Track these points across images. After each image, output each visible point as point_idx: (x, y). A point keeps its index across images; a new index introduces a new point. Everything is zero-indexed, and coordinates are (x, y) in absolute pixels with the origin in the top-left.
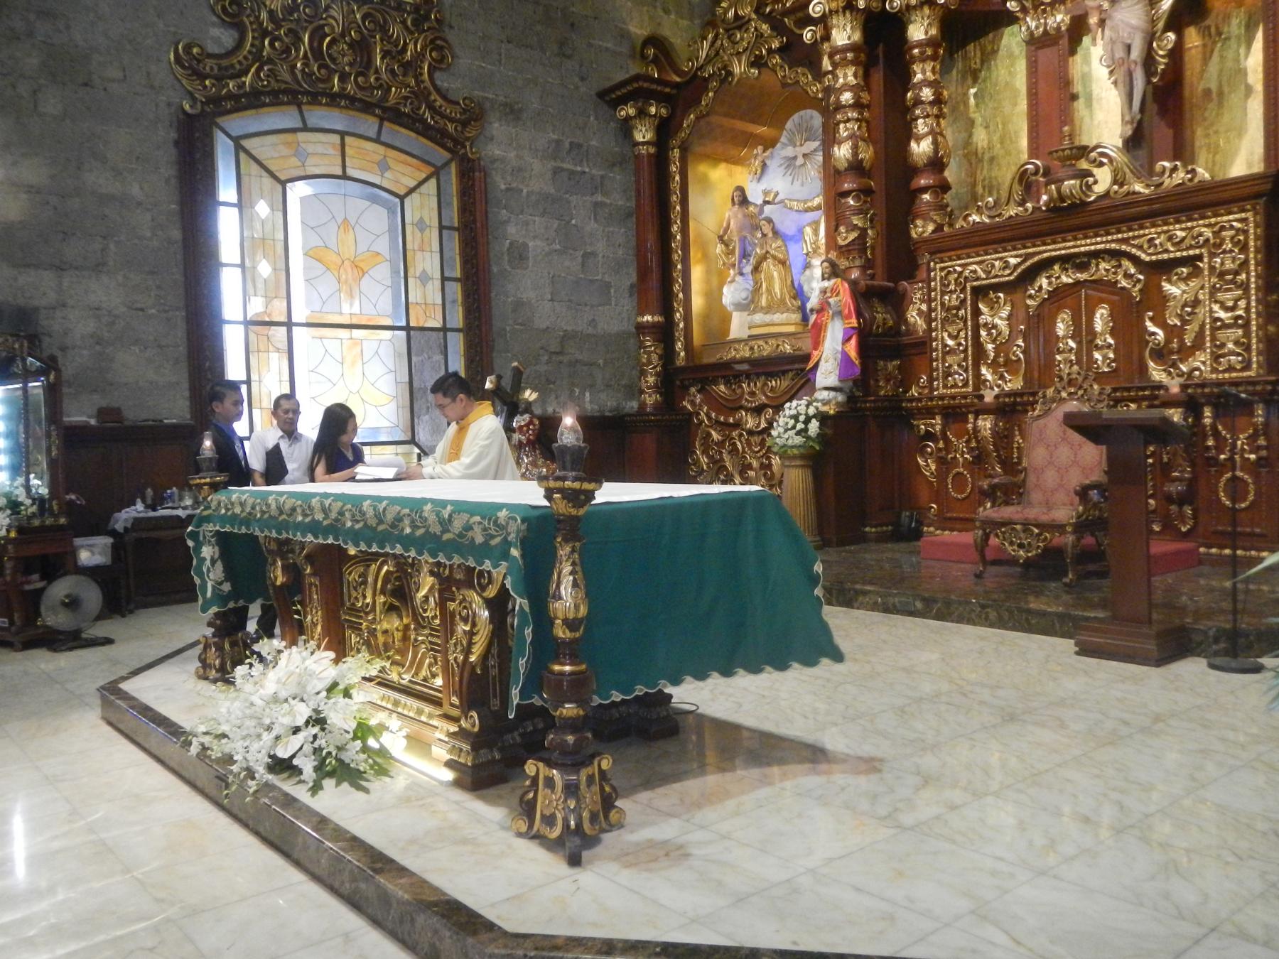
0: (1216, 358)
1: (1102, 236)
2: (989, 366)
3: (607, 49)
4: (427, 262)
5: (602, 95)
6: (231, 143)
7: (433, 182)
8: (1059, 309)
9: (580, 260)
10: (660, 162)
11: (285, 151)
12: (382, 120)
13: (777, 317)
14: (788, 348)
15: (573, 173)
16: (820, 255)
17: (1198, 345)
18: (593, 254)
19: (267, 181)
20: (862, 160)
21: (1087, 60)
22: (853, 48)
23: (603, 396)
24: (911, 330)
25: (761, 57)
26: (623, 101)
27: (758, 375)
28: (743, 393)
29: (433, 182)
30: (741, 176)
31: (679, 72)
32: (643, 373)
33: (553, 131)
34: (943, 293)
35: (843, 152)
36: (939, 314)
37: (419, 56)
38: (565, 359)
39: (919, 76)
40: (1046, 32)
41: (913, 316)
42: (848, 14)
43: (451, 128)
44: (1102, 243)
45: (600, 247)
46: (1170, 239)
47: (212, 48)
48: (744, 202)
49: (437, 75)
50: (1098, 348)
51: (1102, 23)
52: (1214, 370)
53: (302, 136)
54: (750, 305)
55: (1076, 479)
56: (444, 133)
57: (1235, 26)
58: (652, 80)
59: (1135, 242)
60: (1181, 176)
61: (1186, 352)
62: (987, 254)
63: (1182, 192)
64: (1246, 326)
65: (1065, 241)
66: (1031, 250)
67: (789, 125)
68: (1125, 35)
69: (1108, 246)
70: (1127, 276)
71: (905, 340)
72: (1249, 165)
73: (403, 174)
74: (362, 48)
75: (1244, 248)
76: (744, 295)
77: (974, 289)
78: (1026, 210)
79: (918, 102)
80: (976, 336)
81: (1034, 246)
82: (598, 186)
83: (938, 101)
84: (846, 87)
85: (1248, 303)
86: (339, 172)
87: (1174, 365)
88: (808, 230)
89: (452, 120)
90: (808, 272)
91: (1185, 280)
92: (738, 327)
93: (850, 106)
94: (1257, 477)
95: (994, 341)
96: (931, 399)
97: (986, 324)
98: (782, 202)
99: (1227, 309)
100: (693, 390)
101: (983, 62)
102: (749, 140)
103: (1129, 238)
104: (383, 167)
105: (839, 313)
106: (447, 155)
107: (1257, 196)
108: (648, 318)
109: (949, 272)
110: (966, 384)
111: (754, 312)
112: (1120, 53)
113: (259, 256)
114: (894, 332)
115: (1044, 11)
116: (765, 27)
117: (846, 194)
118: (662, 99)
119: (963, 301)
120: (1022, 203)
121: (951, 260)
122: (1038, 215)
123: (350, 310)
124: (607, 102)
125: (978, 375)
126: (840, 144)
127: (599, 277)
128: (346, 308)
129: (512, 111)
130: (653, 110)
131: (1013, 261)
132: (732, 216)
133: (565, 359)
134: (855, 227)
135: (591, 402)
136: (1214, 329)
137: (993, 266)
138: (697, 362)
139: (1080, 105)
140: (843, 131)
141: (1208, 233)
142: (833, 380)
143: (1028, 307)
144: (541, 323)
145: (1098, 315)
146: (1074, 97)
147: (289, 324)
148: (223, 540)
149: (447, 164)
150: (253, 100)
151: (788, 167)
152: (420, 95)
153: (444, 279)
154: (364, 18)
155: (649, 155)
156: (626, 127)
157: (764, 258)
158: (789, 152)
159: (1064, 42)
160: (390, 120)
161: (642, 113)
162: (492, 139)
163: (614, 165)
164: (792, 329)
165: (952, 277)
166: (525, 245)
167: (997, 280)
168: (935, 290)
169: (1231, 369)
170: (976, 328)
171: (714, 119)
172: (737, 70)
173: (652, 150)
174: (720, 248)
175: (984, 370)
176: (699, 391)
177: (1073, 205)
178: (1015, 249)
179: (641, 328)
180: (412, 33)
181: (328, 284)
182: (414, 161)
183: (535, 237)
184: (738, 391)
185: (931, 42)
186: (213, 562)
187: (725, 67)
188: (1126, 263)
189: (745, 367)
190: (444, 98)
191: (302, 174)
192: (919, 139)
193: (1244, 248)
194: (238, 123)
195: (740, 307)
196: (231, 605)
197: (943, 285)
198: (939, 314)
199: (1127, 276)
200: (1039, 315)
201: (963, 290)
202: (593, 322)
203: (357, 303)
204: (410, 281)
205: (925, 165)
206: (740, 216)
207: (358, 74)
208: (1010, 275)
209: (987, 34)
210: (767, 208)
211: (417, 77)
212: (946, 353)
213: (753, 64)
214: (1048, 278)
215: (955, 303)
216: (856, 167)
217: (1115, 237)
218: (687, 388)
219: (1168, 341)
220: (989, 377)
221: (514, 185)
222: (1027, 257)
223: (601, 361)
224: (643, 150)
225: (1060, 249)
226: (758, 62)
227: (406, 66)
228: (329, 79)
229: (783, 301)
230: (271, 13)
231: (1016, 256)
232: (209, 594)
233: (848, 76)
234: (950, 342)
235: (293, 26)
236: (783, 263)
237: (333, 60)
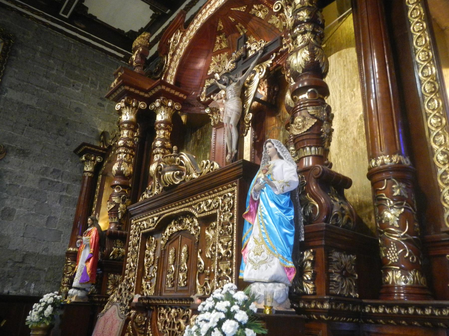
3: (84, 135)
5: (75, 151)
9: (46, 219)
18: (55, 218)
20: (122, 171)
32: (64, 276)
33: (45, 164)
42: (128, 107)
45: (59, 215)
66: (161, 213)
82: (67, 189)
85: (232, 244)
93: (122, 146)
101: (201, 136)
107: (238, 177)
127: (56, 228)
133: (24, 266)
135: (34, 289)
144: (12, 247)
155: (89, 177)
161: (87, 159)
162: (8, 162)
163: (77, 180)
166: (14, 210)
173: (90, 175)
183: (20, 207)
185: (165, 122)
221: (15, 183)
222: (159, 217)
223: (46, 269)
225: (172, 211)
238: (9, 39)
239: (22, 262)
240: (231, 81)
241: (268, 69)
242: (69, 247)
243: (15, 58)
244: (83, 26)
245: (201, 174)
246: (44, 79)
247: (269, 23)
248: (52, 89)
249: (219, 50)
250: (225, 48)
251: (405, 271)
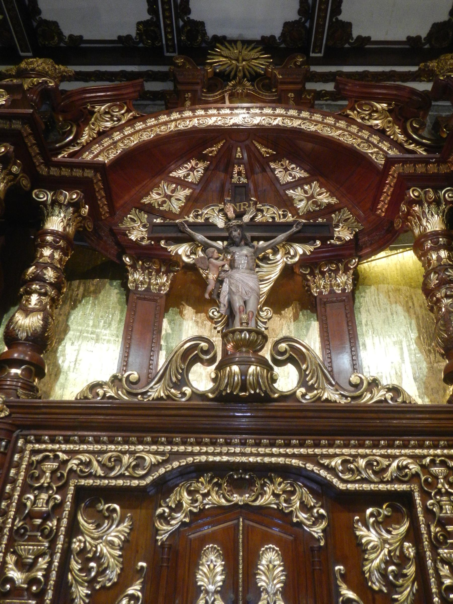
1: (280, 446)
8: (204, 540)
34: (27, 488)
44: (280, 455)
46: (369, 465)
59: (326, 462)
62: (111, 442)
63: (380, 410)
65: (228, 444)
69: (288, 461)
70: (305, 507)
77: (79, 489)
78: (184, 394)
79: (39, 278)
80: (64, 567)
81: (184, 443)
83: (57, 286)
91: (385, 524)
95: (91, 582)
97: (83, 551)
103: (315, 455)
109: (46, 458)
115: (150, 274)
120: (178, 385)
121: (53, 441)
131: (150, 459)
137: (119, 460)
141: (414, 468)
143: (157, 531)
145: (264, 562)
159: (162, 302)
167: (120, 482)
168: (14, 481)
178: (155, 442)
192: (27, 312)
197: (30, 476)
200: (170, 547)
201: (62, 489)
205: (27, 338)
208: (143, 477)
209: (94, 278)
214: (190, 493)
217: (296, 451)
231: (156, 453)
234: (15, 574)
240: (243, 243)
245: (353, 398)
247: (287, 195)
249: (179, 178)
250: (192, 183)
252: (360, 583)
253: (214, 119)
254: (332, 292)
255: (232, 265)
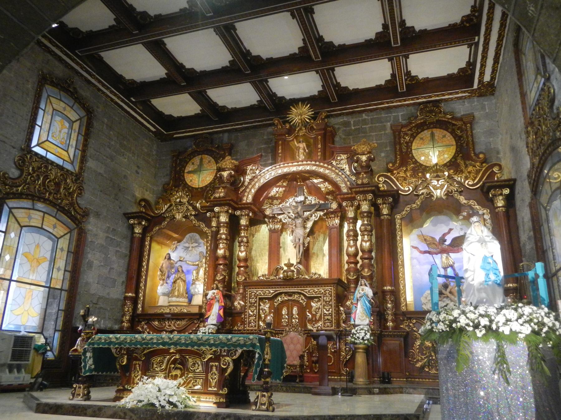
0: (325, 323)
2: (262, 321)
3: (128, 199)
4: (61, 263)
5: (125, 214)
6: (8, 209)
7: (69, 234)
8: (283, 306)
9: (108, 270)
10: (142, 241)
11: (24, 215)
12: (58, 210)
13: (181, 300)
14: (185, 311)
15: (112, 239)
16: (199, 281)
17: (320, 319)
18: (113, 268)
19: (17, 225)
21: (284, 239)
22: (226, 223)
23: (107, 322)
24: (235, 308)
25: (188, 215)
26: (134, 218)
27: (173, 319)
28: (165, 326)
29: (69, 234)
30: (166, 251)
31: (154, 213)
32: (124, 315)
34: (250, 298)
35: (221, 252)
36: (248, 304)
37: (74, 191)
38: (98, 306)
39: (243, 235)
40: (275, 229)
41: (236, 303)
43: (79, 217)
45: (115, 266)
47: (11, 176)
48: (169, 258)
49: (78, 198)
50: (294, 318)
51: (292, 231)
52: (324, 327)
53: (32, 211)
54: (169, 294)
55: (295, 354)
56: (76, 219)
57: (321, 238)
58: (142, 212)
60: (317, 276)
61: (317, 321)
64: (332, 316)
67: (188, 236)
68: (298, 236)
70: (302, 299)
71: (234, 311)
72: (324, 274)
73: (60, 230)
74: (58, 185)
75: (331, 296)
76: (167, 290)
77: (260, 299)
79: (242, 241)
80: (259, 312)
82: (118, 245)
83: (248, 242)
84: (223, 234)
86: (40, 226)
87: (314, 325)
88: (194, 272)
89: (80, 215)
90: (194, 286)
91: (317, 302)
92: (162, 301)
94: (334, 356)
95: (264, 314)
96: (245, 330)
98: (186, 261)
99: (327, 311)
100: (143, 323)
102: (170, 238)
104: (55, 227)
105: (218, 301)
106: (75, 226)
107: (333, 284)
108: (130, 294)
110: (255, 326)
111: (172, 297)
112: (297, 240)
113: (6, 253)
114: (230, 308)
116: (190, 208)
117: (221, 264)
118: (147, 220)
119: (256, 301)
122: (279, 280)
123: (32, 278)
124: (126, 217)
125: (259, 324)
126: (220, 249)
128: (31, 277)
129: (97, 214)
130: (143, 223)
131: (272, 291)
132: (162, 262)
133: (98, 306)
134: (223, 275)
136: (324, 316)
138: (145, 312)
139: (282, 250)
140: (221, 246)
142: (215, 322)
144: (92, 292)
146: (281, 247)
147: (10, 280)
148: (94, 350)
149: (74, 229)
150: (19, 196)
151: (185, 250)
152: (72, 204)
153: (65, 271)
154: (61, 175)
156: (132, 227)
157: (178, 279)
158: (187, 245)
160: (61, 211)
161: (140, 223)
162: (89, 223)
164: (185, 304)
165: (253, 294)
166: (93, 262)
169: (328, 326)
170: (259, 309)
171: (165, 230)
172: (177, 217)
174: (159, 273)
175: (260, 323)
176: (146, 324)
177: (290, 279)
179: (126, 298)
180: (73, 183)
181: (27, 267)
182: (64, 226)
184: (164, 324)
185: (246, 226)
186: (90, 358)
187: (173, 216)
188: (302, 296)
189: (170, 316)
190: (79, 207)
191: (28, 225)
192: (242, 252)
193: (331, 296)
194: (12, 203)
195: (164, 294)
196: (94, 373)
198: (248, 304)
199: (302, 299)
201: (256, 298)
202: (108, 294)
203: (35, 275)
204: (54, 269)
206: (167, 263)
207: (55, 194)
210: (179, 264)
211: (72, 198)
212: (249, 317)
213: (184, 217)
215: (253, 302)
216: (224, 257)
218: (141, 322)
219: (312, 318)
220: (262, 325)
224: (138, 235)
226: (186, 217)
227: (70, 193)
228: (45, 194)
229: (183, 294)
230: (33, 168)
232: (87, 368)
233: (223, 230)
235: (39, 173)
236: (184, 281)
237: (48, 187)
238: (91, 113)
239: (96, 304)
241: (320, 216)
242: (128, 293)
243: (92, 130)
244: (141, 108)
246: (108, 149)
248: (112, 158)
251: (393, 322)
252: (310, 313)
253: (286, 169)
254: (333, 225)
255: (295, 226)
